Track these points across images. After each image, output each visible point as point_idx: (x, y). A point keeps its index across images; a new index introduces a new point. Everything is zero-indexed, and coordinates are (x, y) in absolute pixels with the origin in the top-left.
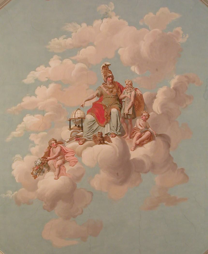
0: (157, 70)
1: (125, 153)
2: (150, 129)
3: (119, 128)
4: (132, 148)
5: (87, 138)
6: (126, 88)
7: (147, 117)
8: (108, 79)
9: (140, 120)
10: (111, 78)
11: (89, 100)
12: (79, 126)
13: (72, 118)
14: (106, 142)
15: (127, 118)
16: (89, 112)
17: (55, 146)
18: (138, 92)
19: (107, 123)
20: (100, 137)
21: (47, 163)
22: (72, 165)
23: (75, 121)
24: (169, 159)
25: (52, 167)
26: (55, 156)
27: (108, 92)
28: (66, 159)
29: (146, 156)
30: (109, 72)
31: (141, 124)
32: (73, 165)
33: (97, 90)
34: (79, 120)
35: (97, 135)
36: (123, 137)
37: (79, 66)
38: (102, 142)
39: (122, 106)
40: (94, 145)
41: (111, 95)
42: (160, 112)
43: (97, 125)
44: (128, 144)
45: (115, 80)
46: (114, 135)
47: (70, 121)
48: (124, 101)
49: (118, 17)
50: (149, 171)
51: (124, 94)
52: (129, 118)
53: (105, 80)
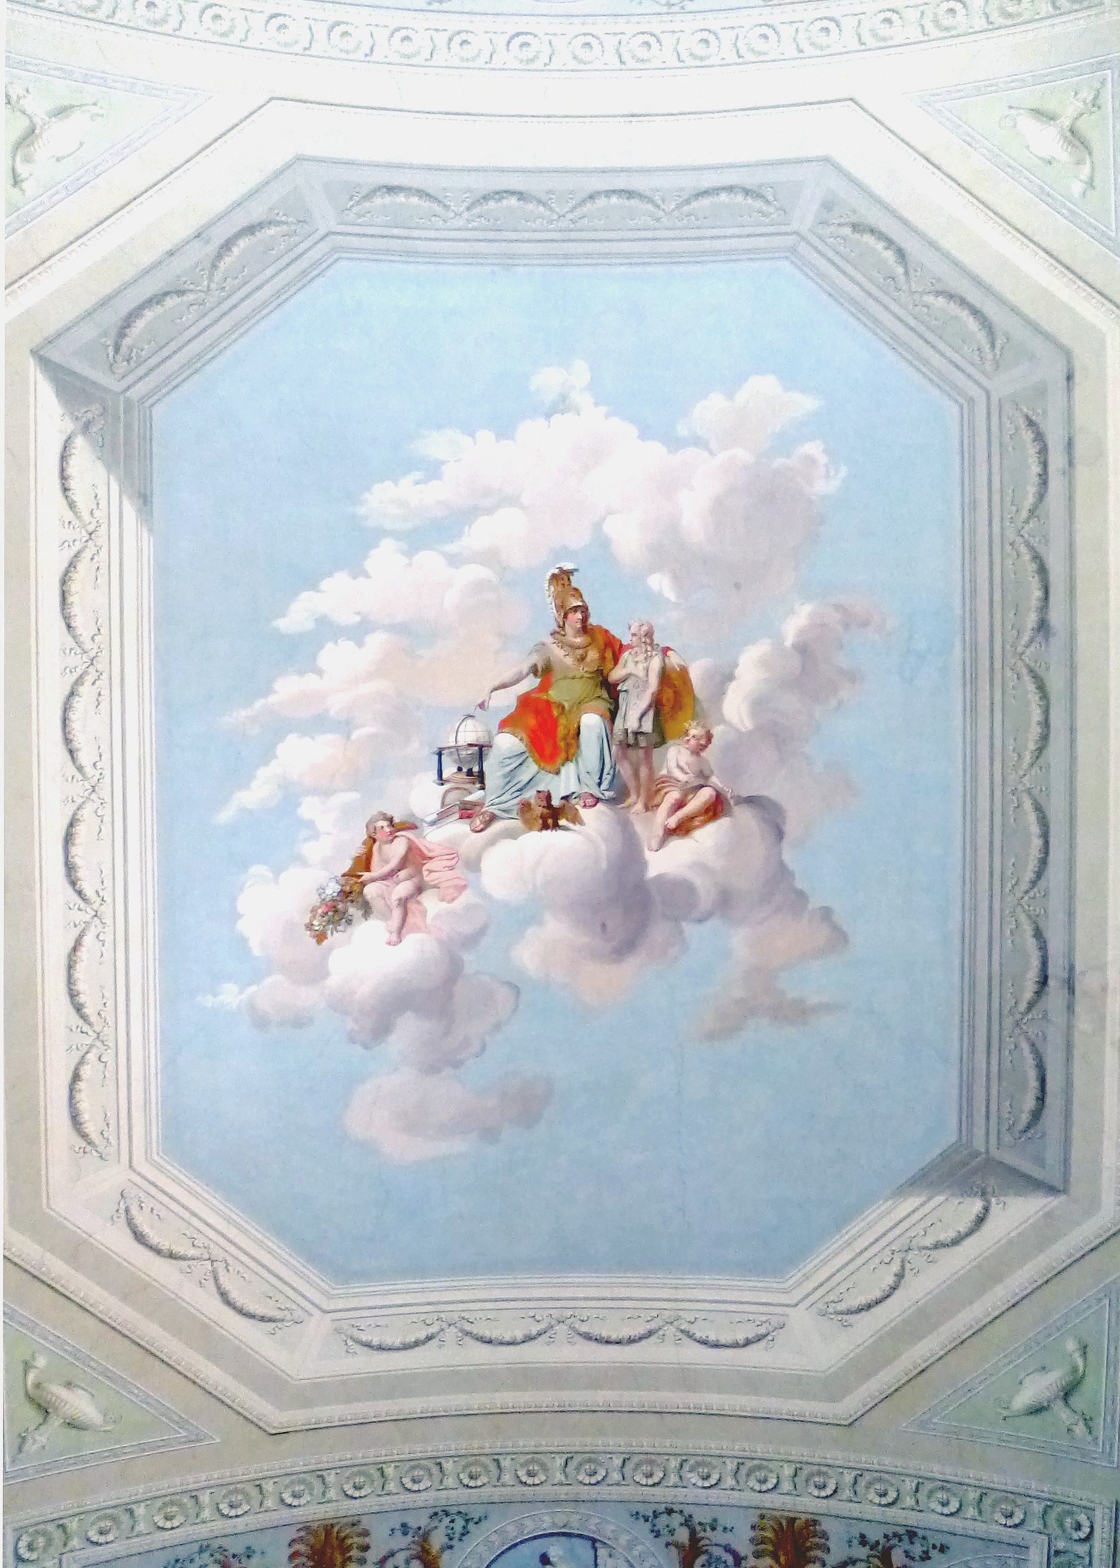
0: (737, 586)
2: (714, 780)
4: (655, 845)
6: (630, 647)
7: (703, 742)
8: (570, 616)
11: (504, 686)
12: (470, 773)
15: (636, 745)
16: (504, 724)
18: (674, 660)
19: (567, 759)
21: (361, 892)
22: (449, 897)
24: (781, 874)
25: (377, 904)
26: (387, 868)
27: (569, 661)
29: (701, 867)
31: (682, 764)
35: (532, 801)
39: (617, 707)
41: (582, 670)
42: (748, 724)
43: (531, 768)
44: (639, 828)
45: (593, 621)
46: (590, 801)
47: (440, 754)
48: (624, 689)
49: (603, 409)
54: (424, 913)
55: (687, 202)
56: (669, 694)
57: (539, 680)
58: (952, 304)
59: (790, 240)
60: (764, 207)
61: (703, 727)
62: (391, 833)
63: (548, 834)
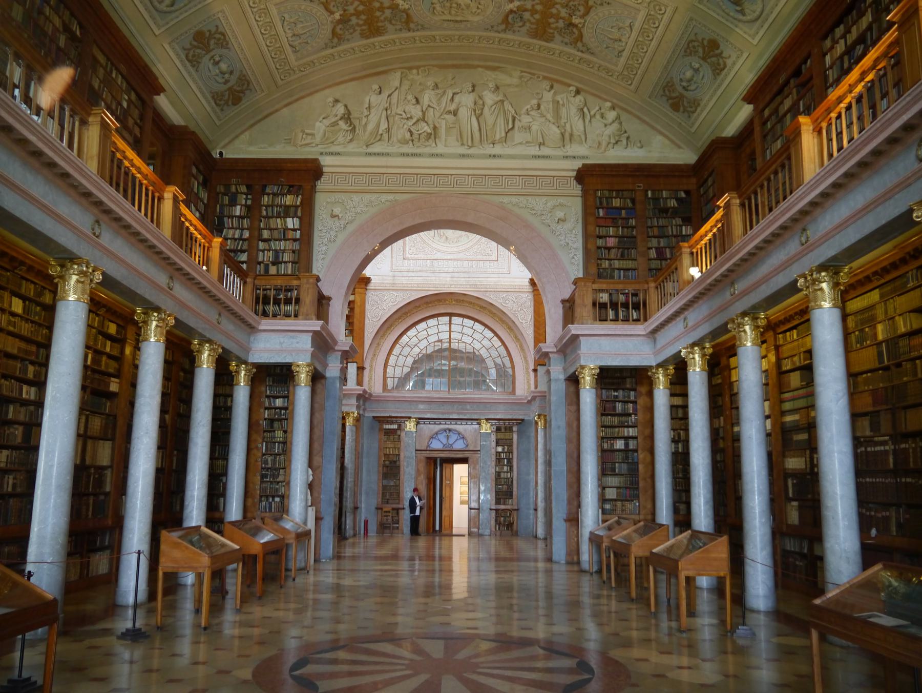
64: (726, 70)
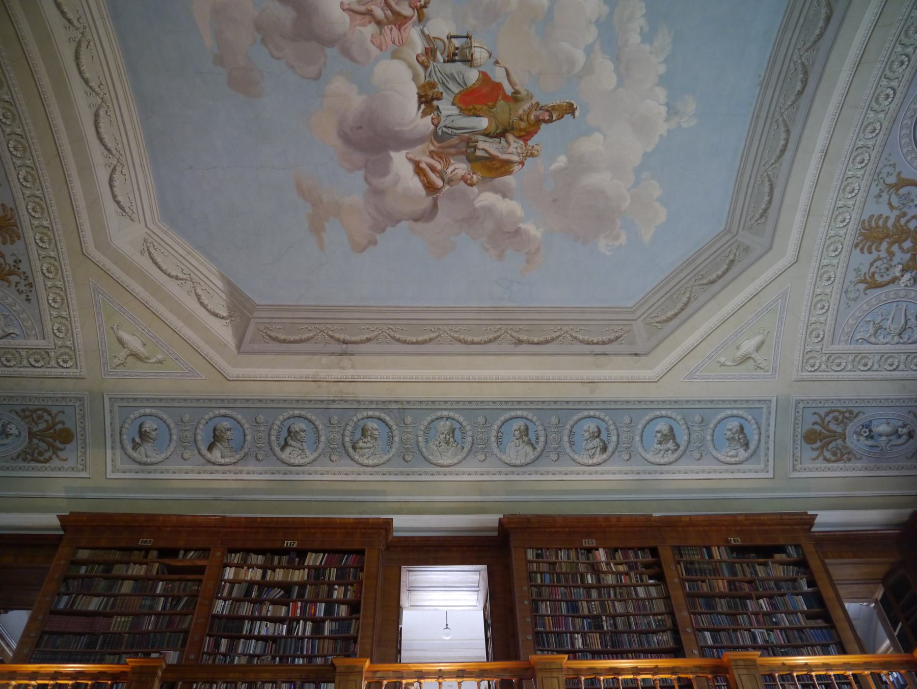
0: (555, 201)
1: (402, 142)
2: (447, 187)
3: (449, 131)
5: (431, 71)
6: (526, 145)
7: (469, 182)
8: (547, 113)
9: (464, 169)
10: (547, 118)
12: (455, 54)
13: (473, 40)
14: (423, 106)
16: (484, 77)
17: (413, 6)
18: (516, 168)
19: (461, 110)
20: (432, 96)
23: (466, 48)
24: (393, 219)
27: (521, 112)
28: (386, 27)
30: (559, 115)
31: (456, 171)
32: (375, 42)
33: (527, 90)
34: (468, 55)
35: (436, 90)
36: (433, 139)
37: (580, 57)
38: (423, 99)
39: (491, 137)
40: (416, 84)
41: (514, 119)
43: (456, 90)
44: (419, 148)
45: (543, 126)
46: (436, 121)
47: (467, 37)
48: (502, 142)
50: (369, 184)
51: (515, 142)
52: (469, 151)
53: (544, 106)
54: (363, 25)
55: (770, 180)
56: (498, 164)
57: (510, 95)
58: (682, 305)
59: (734, 230)
60: (755, 218)
61: (477, 182)
62: (416, 7)
63: (416, 98)
64: (40, 465)
